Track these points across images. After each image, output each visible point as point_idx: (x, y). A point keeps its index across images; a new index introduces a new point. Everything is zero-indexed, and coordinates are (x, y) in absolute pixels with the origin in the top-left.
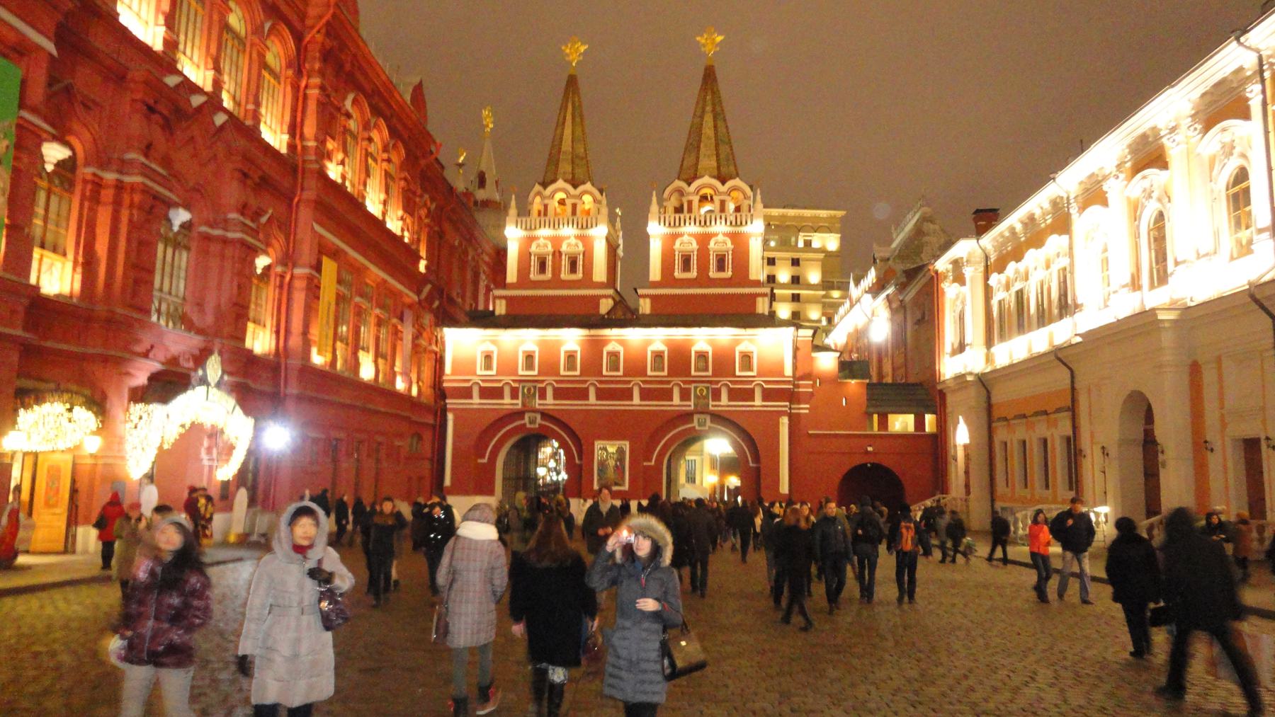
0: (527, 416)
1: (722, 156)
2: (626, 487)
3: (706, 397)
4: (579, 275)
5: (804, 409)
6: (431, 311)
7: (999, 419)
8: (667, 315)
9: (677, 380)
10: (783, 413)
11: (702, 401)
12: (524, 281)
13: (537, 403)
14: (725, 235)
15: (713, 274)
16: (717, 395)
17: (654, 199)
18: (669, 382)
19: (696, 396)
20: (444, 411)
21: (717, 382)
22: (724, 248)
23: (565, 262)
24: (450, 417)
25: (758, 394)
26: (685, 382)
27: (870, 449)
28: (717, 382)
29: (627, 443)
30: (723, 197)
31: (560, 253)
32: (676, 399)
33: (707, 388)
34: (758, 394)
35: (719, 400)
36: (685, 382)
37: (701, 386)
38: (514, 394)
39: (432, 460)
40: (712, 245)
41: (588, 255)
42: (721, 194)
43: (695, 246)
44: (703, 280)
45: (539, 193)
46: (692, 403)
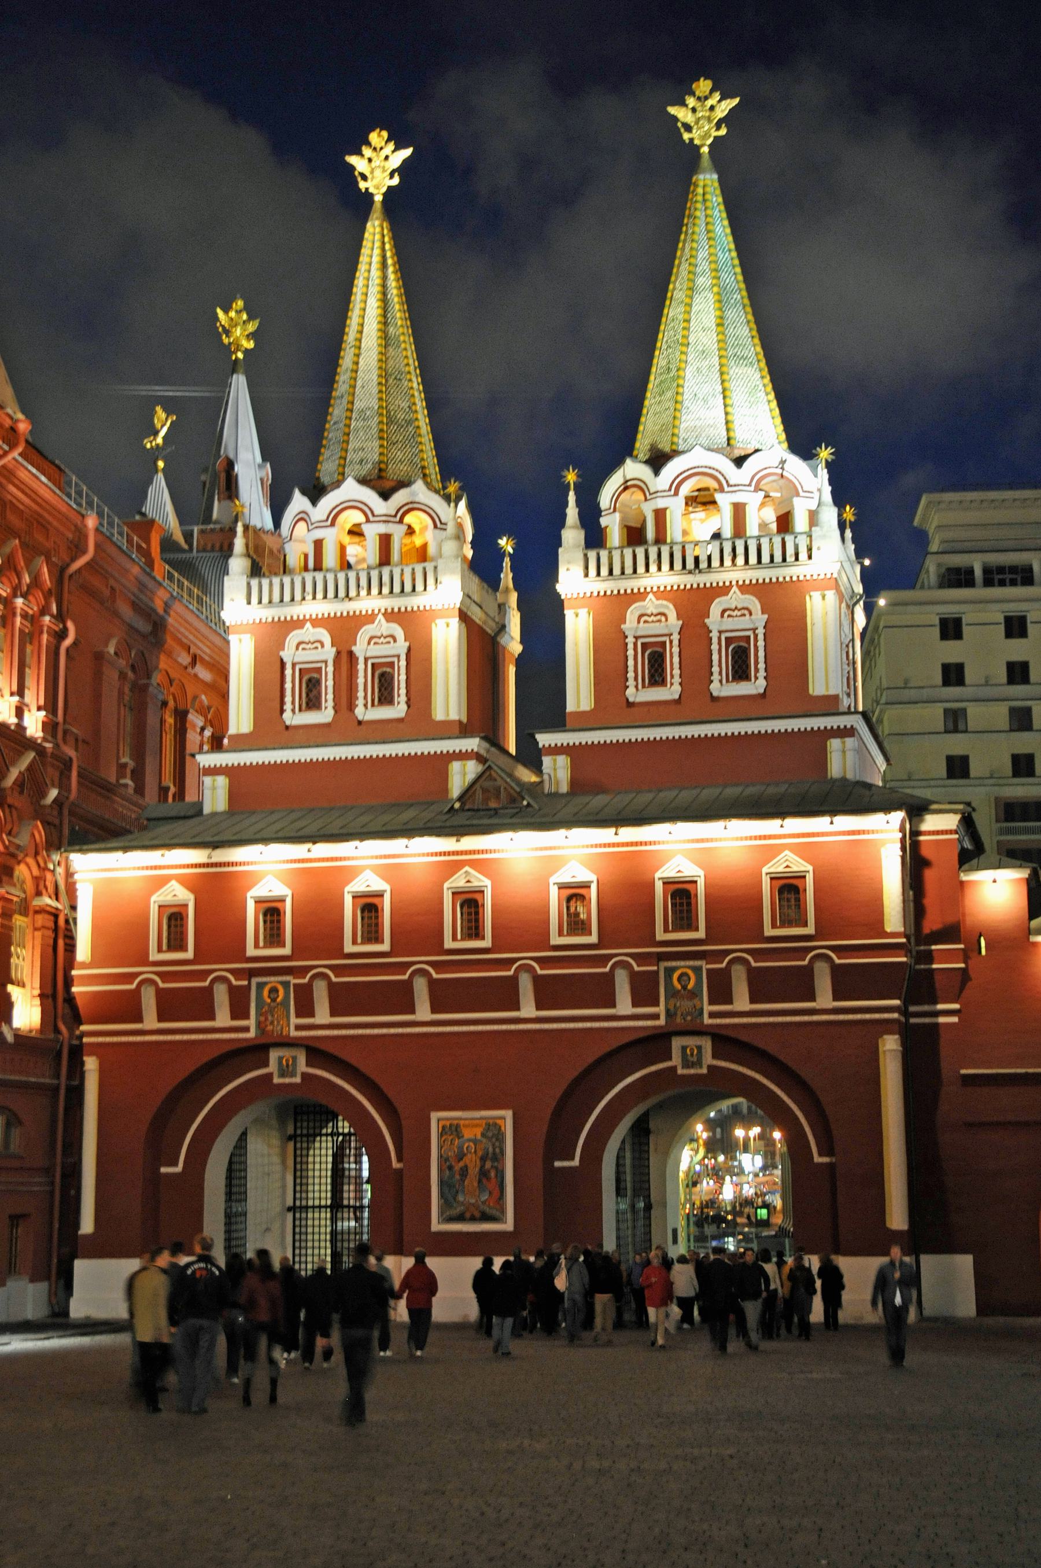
0: (274, 1055)
3: (695, 994)
4: (398, 710)
6: (38, 813)
8: (617, 789)
10: (886, 1027)
11: (686, 1005)
12: (269, 729)
13: (293, 1025)
14: (745, 588)
15: (721, 687)
16: (721, 991)
17: (572, 512)
18: (604, 959)
19: (671, 994)
20: (77, 1053)
22: (744, 622)
24: (91, 1064)
26: (639, 958)
29: (508, 1114)
30: (739, 498)
31: (352, 656)
32: (624, 1005)
33: (697, 970)
35: (311, 1014)
36: (639, 958)
37: (682, 966)
38: (239, 1010)
39: (48, 1171)
40: (714, 620)
41: (419, 657)
42: (735, 487)
43: (674, 622)
44: (697, 702)
45: (303, 517)
46: (661, 1009)
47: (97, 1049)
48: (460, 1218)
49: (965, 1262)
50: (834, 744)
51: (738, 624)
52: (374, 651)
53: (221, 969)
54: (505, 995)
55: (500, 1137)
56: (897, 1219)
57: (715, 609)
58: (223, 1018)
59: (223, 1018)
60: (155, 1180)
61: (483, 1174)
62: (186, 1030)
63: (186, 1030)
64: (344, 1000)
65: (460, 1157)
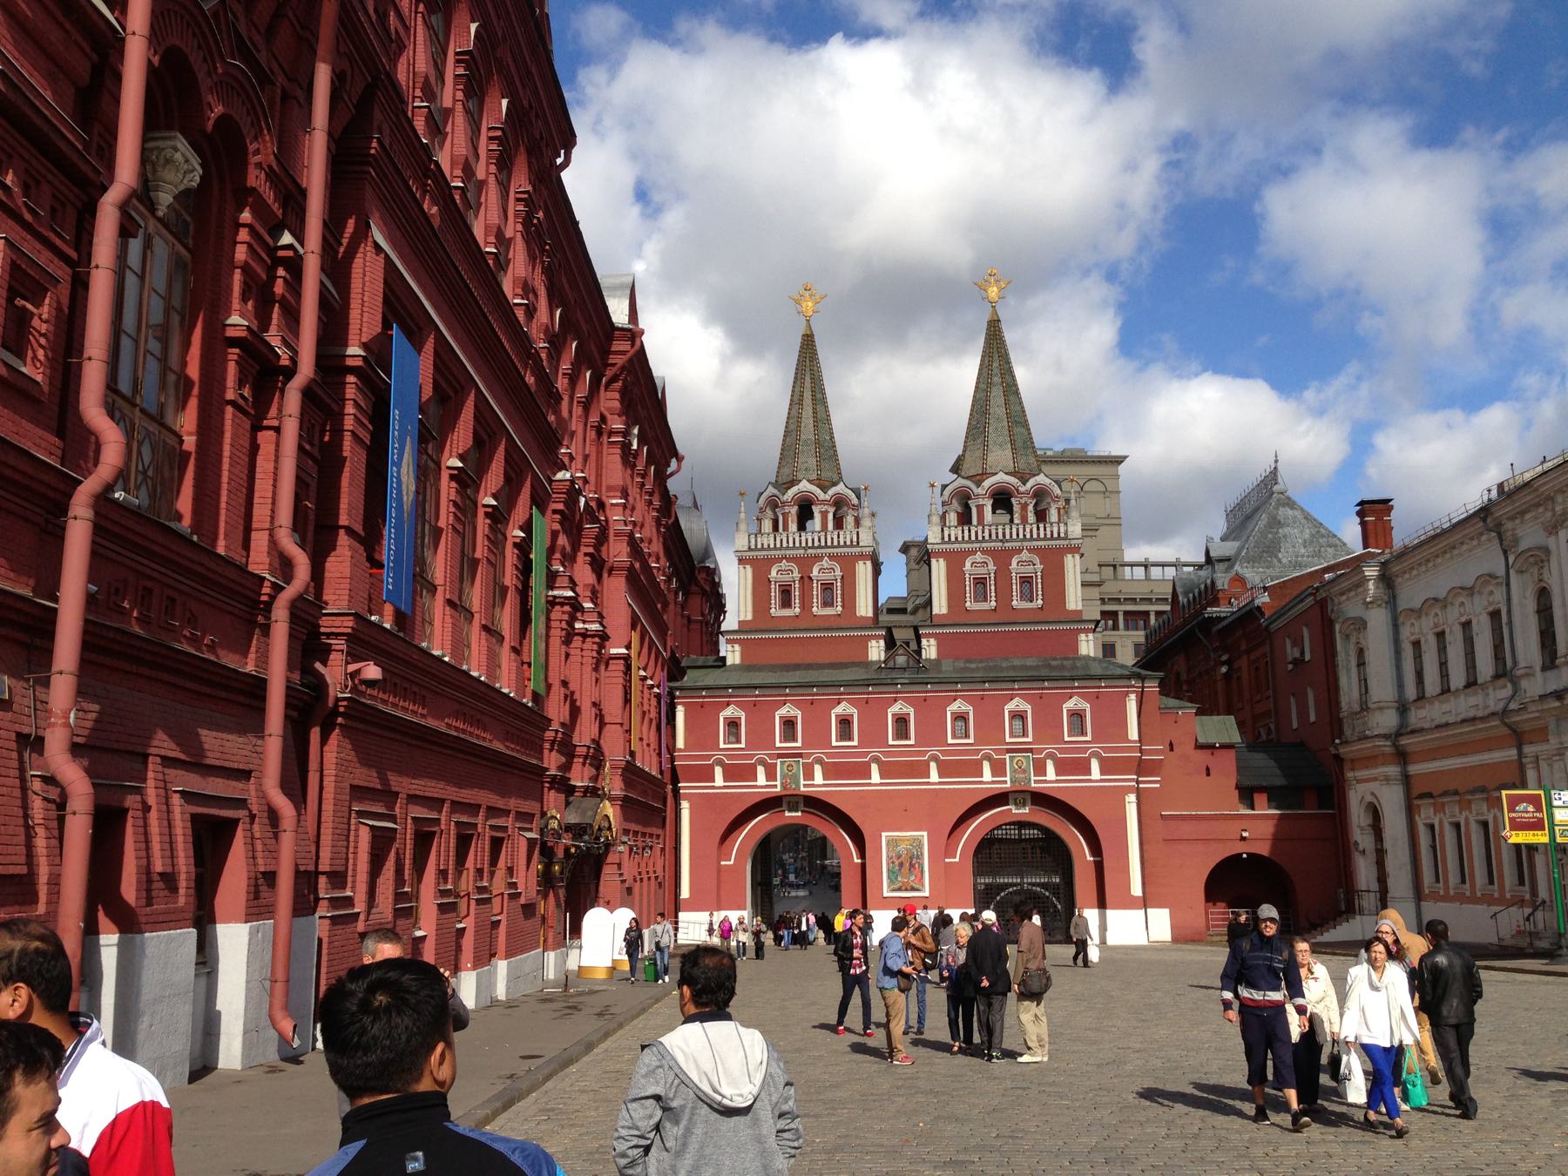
1: (1019, 444)
2: (927, 894)
5: (1151, 783)
7: (1422, 796)
9: (987, 749)
16: (1040, 769)
19: (1014, 771)
21: (1040, 751)
23: (816, 590)
24: (685, 805)
25: (1095, 765)
27: (1245, 834)
28: (1040, 751)
32: (987, 775)
34: (1095, 765)
38: (771, 775)
47: (689, 797)
48: (899, 889)
49: (1166, 911)
50: (1083, 637)
51: (1028, 570)
52: (823, 576)
53: (761, 754)
54: (921, 770)
55: (920, 846)
56: (1136, 889)
57: (1014, 562)
58: (761, 779)
59: (761, 779)
60: (719, 869)
61: (912, 866)
62: (740, 788)
63: (740, 788)
64: (831, 771)
65: (899, 857)
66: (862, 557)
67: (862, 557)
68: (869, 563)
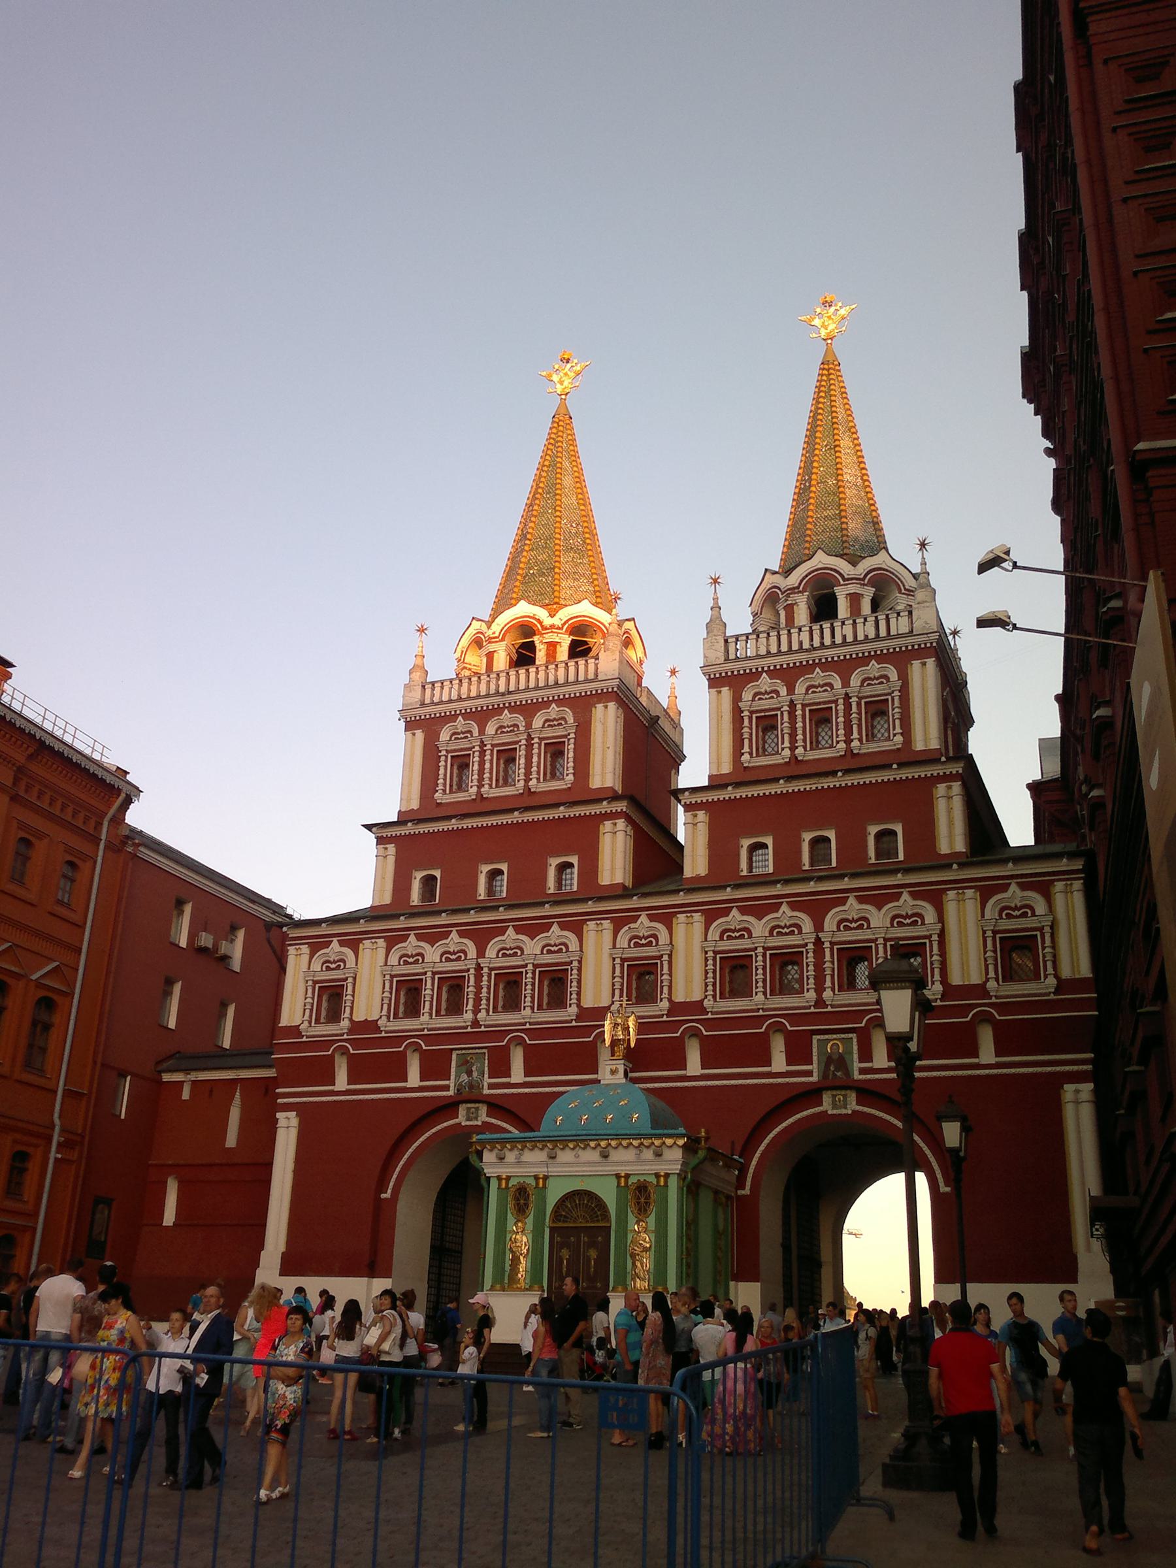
66: (603, 696)
67: (603, 696)
68: (612, 706)
